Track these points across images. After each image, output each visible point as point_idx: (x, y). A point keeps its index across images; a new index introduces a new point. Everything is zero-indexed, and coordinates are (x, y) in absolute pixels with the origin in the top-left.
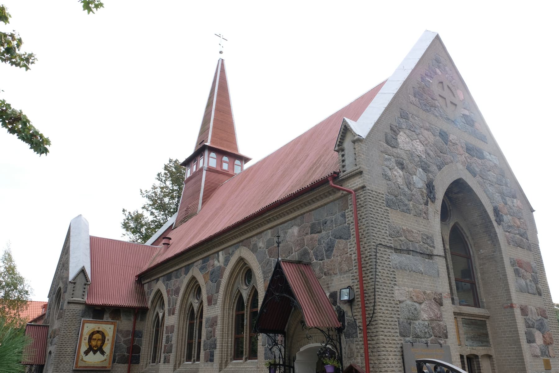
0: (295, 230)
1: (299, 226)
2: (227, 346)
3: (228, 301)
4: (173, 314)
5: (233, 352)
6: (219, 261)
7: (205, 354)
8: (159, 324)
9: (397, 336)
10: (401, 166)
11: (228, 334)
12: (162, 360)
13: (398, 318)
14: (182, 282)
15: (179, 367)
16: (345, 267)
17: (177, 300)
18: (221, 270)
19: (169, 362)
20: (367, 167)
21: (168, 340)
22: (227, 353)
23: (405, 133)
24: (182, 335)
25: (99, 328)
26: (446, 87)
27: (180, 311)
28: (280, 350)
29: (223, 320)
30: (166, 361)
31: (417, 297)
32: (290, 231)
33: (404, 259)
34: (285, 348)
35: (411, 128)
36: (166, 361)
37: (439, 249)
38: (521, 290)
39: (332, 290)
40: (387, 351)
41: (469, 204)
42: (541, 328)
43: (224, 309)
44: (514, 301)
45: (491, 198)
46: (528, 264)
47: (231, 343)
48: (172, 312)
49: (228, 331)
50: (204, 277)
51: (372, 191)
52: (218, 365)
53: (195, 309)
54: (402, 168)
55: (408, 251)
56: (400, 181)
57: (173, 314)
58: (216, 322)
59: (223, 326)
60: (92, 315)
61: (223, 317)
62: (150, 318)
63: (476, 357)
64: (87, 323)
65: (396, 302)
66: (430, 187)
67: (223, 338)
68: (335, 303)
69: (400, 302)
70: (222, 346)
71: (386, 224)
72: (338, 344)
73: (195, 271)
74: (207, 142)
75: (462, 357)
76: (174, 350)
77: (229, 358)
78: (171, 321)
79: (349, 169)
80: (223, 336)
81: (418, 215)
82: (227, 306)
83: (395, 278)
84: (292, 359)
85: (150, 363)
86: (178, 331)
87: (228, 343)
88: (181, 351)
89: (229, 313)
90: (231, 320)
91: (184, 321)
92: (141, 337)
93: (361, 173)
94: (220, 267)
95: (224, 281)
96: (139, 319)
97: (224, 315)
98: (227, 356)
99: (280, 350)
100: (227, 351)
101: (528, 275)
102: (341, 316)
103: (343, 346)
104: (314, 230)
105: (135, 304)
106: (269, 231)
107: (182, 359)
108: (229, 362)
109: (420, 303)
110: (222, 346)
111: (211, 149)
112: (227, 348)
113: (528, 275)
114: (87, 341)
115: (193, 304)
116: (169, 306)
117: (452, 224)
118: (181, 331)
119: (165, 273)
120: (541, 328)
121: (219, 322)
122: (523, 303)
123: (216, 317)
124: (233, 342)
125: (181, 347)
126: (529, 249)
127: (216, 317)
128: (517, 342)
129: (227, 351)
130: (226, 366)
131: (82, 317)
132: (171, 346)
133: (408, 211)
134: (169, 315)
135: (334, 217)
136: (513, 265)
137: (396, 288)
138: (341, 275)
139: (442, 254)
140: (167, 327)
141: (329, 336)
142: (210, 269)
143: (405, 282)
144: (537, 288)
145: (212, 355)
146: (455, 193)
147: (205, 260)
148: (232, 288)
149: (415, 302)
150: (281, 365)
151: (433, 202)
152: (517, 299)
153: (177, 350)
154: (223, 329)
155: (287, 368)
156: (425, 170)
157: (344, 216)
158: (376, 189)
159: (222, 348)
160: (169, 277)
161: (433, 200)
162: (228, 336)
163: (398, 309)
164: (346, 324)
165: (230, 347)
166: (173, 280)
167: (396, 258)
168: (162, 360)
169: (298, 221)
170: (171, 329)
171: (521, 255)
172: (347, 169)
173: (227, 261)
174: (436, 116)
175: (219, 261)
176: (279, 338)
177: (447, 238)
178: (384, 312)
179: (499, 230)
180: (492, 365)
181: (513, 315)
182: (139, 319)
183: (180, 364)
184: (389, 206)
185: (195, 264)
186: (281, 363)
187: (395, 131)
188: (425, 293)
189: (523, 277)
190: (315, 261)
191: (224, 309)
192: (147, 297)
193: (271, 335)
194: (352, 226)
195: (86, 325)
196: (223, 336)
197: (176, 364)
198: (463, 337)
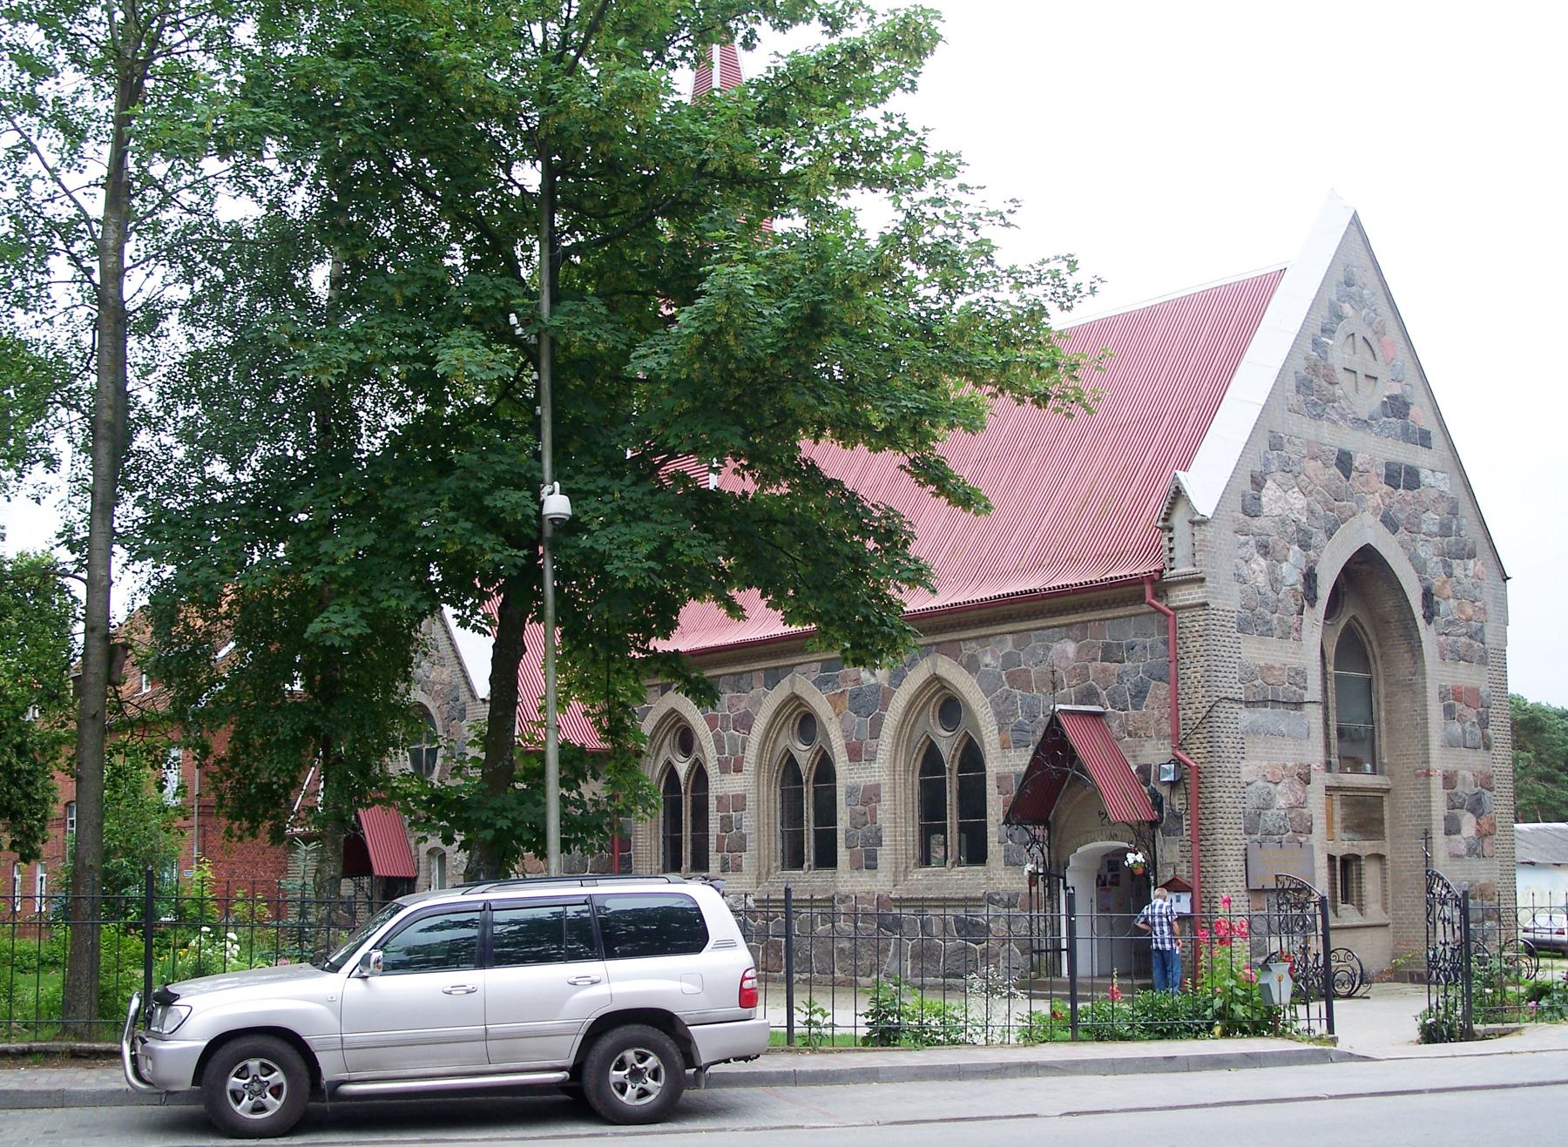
0: (1070, 648)
3: (902, 756)
10: (1264, 549)
17: (744, 741)
31: (1273, 774)
32: (1057, 646)
37: (1314, 691)
38: (1450, 743)
39: (1143, 761)
42: (1476, 807)
44: (1433, 766)
45: (1420, 567)
46: (1475, 692)
54: (1265, 555)
55: (1265, 703)
56: (1262, 580)
57: (738, 770)
63: (1358, 858)
66: (1310, 578)
68: (1147, 782)
75: (1331, 858)
76: (751, 845)
79: (1182, 569)
81: (1285, 636)
82: (901, 767)
93: (1202, 580)
101: (1471, 714)
102: (1157, 802)
104: (1108, 654)
106: (1009, 637)
113: (1471, 714)
116: (720, 748)
117: (1343, 623)
120: (1476, 807)
121: (886, 795)
122: (1451, 767)
126: (1483, 661)
127: (878, 786)
128: (1427, 836)
133: (1269, 632)
135: (1148, 642)
136: (1443, 699)
137: (1243, 763)
139: (1319, 698)
144: (1484, 736)
151: (1312, 606)
152: (1440, 760)
156: (1305, 546)
161: (1312, 599)
167: (1246, 716)
169: (1076, 632)
171: (1466, 676)
173: (898, 678)
174: (1334, 422)
176: (1040, 832)
177: (1331, 652)
178: (1228, 808)
179: (1428, 636)
180: (1383, 871)
181: (1428, 788)
183: (768, 873)
184: (1241, 630)
185: (799, 668)
187: (1258, 482)
188: (1284, 767)
189: (1461, 719)
198: (1338, 826)
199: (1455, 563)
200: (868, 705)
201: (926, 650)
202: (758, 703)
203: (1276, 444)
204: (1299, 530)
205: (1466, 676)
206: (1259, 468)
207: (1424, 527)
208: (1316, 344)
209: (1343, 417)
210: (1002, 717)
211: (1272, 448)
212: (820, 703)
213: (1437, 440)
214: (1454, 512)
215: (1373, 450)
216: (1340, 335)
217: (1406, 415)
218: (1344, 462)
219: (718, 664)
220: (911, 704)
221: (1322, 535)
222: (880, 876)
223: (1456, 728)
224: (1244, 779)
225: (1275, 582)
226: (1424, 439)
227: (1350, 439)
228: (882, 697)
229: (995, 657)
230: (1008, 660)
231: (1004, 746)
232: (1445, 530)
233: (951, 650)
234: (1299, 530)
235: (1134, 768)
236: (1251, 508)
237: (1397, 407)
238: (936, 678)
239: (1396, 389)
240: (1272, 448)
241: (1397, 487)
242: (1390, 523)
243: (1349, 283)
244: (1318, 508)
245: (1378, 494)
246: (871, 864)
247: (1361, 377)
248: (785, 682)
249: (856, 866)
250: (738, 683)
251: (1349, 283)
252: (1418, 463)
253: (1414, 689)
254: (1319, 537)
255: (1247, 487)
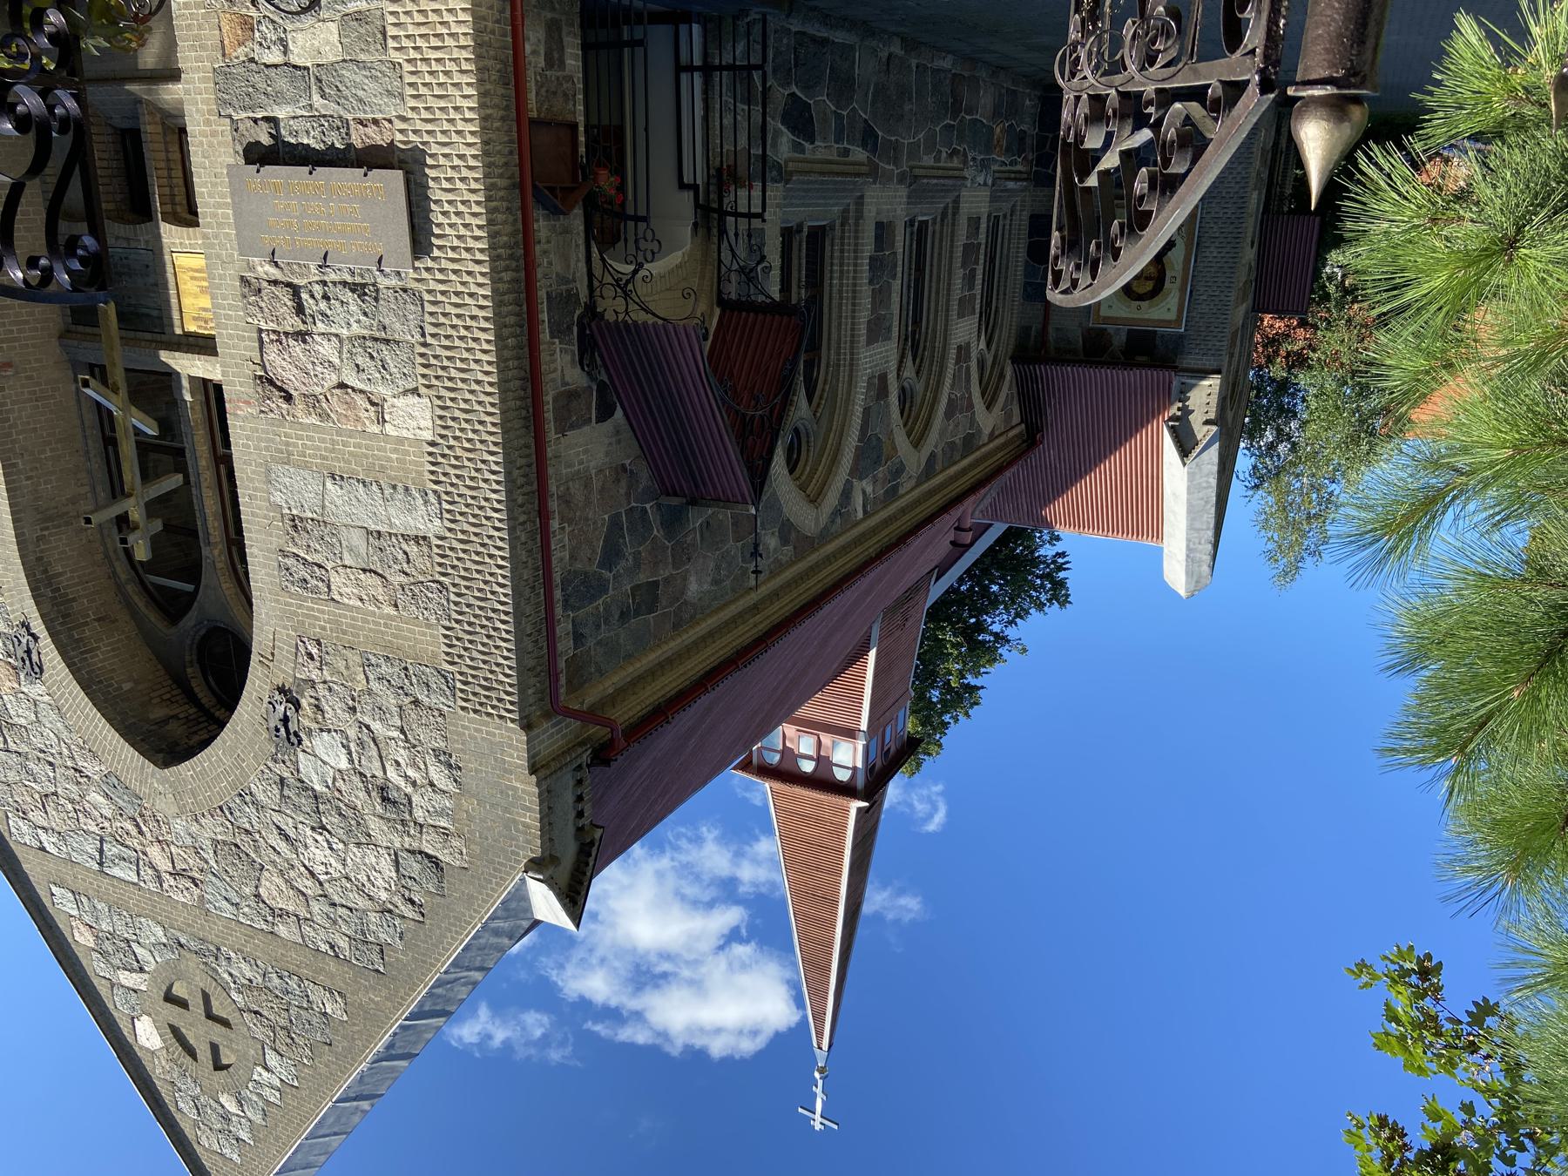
1: (686, 603)
2: (841, 265)
3: (842, 388)
4: (960, 348)
5: (828, 248)
6: (864, 492)
7: (893, 245)
8: (988, 324)
9: (429, 292)
11: (841, 298)
12: (983, 226)
13: (425, 345)
14: (942, 433)
15: (946, 208)
16: (576, 488)
18: (857, 472)
19: (969, 219)
20: (515, 789)
21: (970, 279)
22: (842, 244)
23: (371, 898)
24: (938, 293)
25: (1139, 308)
26: (204, 1054)
27: (943, 357)
28: (734, 255)
29: (853, 336)
30: (974, 222)
31: (350, 405)
34: (720, 261)
36: (974, 222)
40: (468, 250)
41: (127, 686)
43: (851, 365)
47: (831, 272)
48: (963, 352)
49: (840, 305)
50: (894, 448)
51: (501, 717)
52: (866, 214)
53: (910, 358)
57: (960, 348)
58: (869, 330)
59: (853, 317)
60: (1158, 342)
61: (852, 342)
62: (1005, 334)
64: (1170, 321)
65: (432, 392)
67: (855, 285)
69: (415, 391)
70: (855, 265)
71: (457, 621)
72: (597, 272)
73: (913, 460)
74: (859, 810)
76: (959, 253)
77: (838, 233)
78: (965, 330)
80: (854, 292)
83: (433, 464)
84: (701, 232)
85: (1005, 216)
86: (948, 301)
87: (842, 272)
88: (941, 248)
89: (839, 354)
90: (834, 336)
91: (935, 331)
92: (1026, 284)
94: (861, 479)
95: (852, 440)
96: (1033, 333)
97: (852, 348)
98: (842, 238)
99: (734, 255)
100: (842, 251)
103: (582, 266)
105: (1040, 370)
107: (938, 227)
108: (838, 223)
109: (342, 386)
110: (855, 265)
111: (847, 790)
112: (842, 258)
114: (1169, 274)
115: (913, 375)
116: (968, 368)
118: (942, 301)
119: (978, 454)
121: (863, 330)
123: (870, 342)
124: (827, 275)
125: (940, 260)
127: (870, 342)
129: (842, 251)
130: (846, 211)
131: (1181, 336)
132: (964, 265)
134: (968, 344)
135: (604, 634)
137: (428, 435)
138: (587, 469)
141: (626, 295)
142: (881, 471)
143: (395, 451)
145: (879, 240)
146: (175, 717)
148: (831, 422)
149: (361, 391)
150: (731, 214)
153: (951, 252)
154: (854, 311)
155: (715, 205)
157: (578, 638)
158: (486, 724)
159: (856, 258)
162: (840, 292)
163: (425, 371)
164: (575, 329)
165: (836, 261)
168: (983, 226)
170: (965, 307)
172: (569, 776)
173: (846, 495)
175: (864, 492)
182: (1033, 333)
183: (944, 214)
186: (730, 219)
190: (648, 506)
191: (851, 365)
192: (1015, 391)
193: (761, 298)
194: (559, 610)
195: (1172, 316)
196: (854, 292)
197: (954, 214)
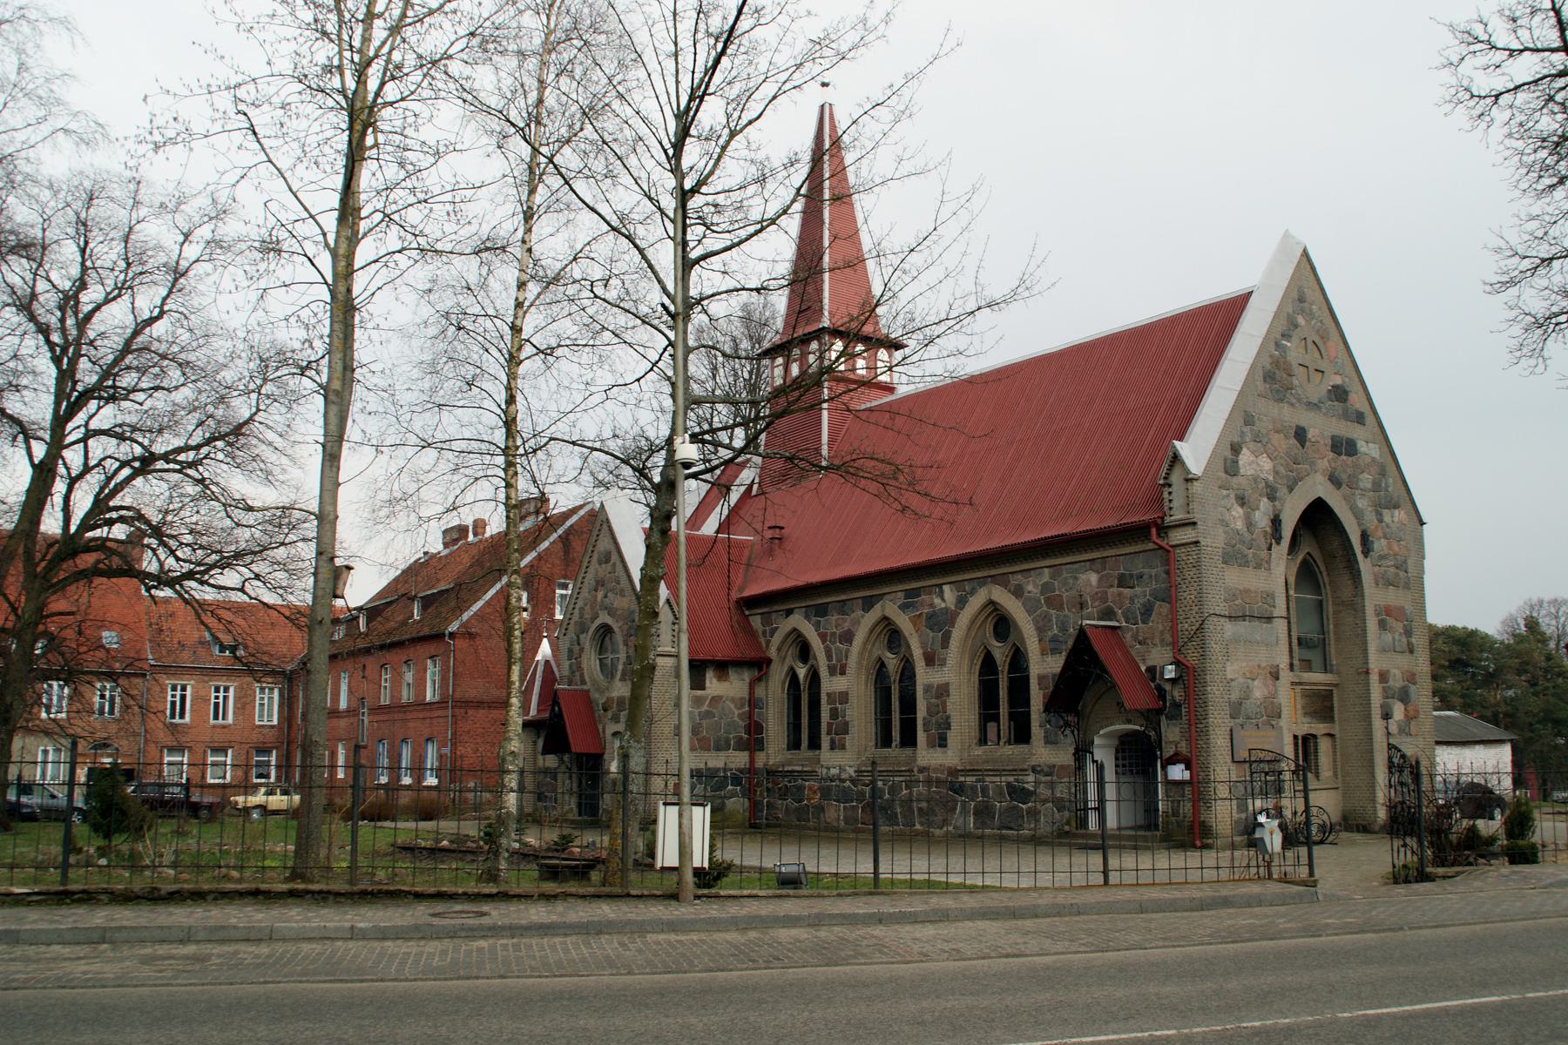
0: (1093, 578)
10: (1242, 501)
17: (847, 651)
32: (1083, 577)
33: (1242, 628)
35: (1257, 439)
37: (1280, 610)
39: (1150, 663)
42: (1404, 697)
44: (1371, 666)
45: (1358, 515)
46: (1401, 609)
48: (839, 669)
54: (1242, 505)
55: (1243, 617)
56: (1240, 525)
57: (843, 673)
63: (1315, 736)
66: (1276, 522)
68: (1153, 679)
75: (1295, 737)
79: (1178, 515)
81: (1258, 566)
101: (1399, 627)
102: (1162, 694)
104: (1123, 582)
116: (829, 657)
117: (1300, 557)
120: (1404, 697)
122: (1385, 667)
126: (1407, 587)
127: (947, 684)
128: (1368, 717)
133: (1246, 564)
135: (1153, 572)
136: (1378, 615)
139: (1284, 614)
140: (829, 695)
144: (1409, 644)
147: (911, 594)
151: (1278, 543)
152: (1375, 662)
156: (1272, 498)
160: (822, 611)
161: (1277, 537)
166: (834, 618)
167: (1230, 628)
169: (1098, 565)
171: (1393, 597)
173: (962, 602)
177: (1292, 580)
178: (1217, 695)
179: (1364, 565)
180: (1334, 747)
181: (1367, 684)
184: (1225, 562)
187: (1236, 449)
189: (1392, 630)
198: (1300, 712)
199: (1385, 512)
200: (940, 623)
201: (982, 582)
202: (857, 622)
203: (1249, 420)
204: (1267, 486)
205: (1393, 597)
206: (1236, 439)
207: (1361, 485)
208: (1277, 345)
209: (1299, 400)
210: (1041, 630)
211: (1246, 423)
212: (904, 622)
213: (1370, 419)
214: (1383, 474)
215: (1321, 427)
216: (1295, 339)
217: (1345, 400)
218: (1300, 435)
219: (828, 594)
220: (973, 622)
221: (1285, 490)
222: (950, 753)
223: (1388, 637)
224: (1229, 677)
225: (1250, 525)
226: (1360, 418)
227: (1306, 418)
228: (949, 618)
229: (1035, 586)
230: (1046, 588)
231: (1043, 653)
232: (1376, 487)
233: (1002, 581)
234: (1267, 486)
235: (1143, 669)
236: (1231, 469)
237: (1339, 393)
238: (991, 602)
239: (1338, 380)
240: (1246, 423)
241: (1340, 454)
242: (1335, 481)
243: (1301, 300)
244: (1282, 470)
245: (1326, 461)
246: (942, 742)
247: (1311, 370)
248: (878, 607)
249: (931, 744)
250: (843, 608)
251: (1301, 300)
252: (1354, 436)
253: (1355, 606)
254: (1282, 491)
255: (1228, 454)
